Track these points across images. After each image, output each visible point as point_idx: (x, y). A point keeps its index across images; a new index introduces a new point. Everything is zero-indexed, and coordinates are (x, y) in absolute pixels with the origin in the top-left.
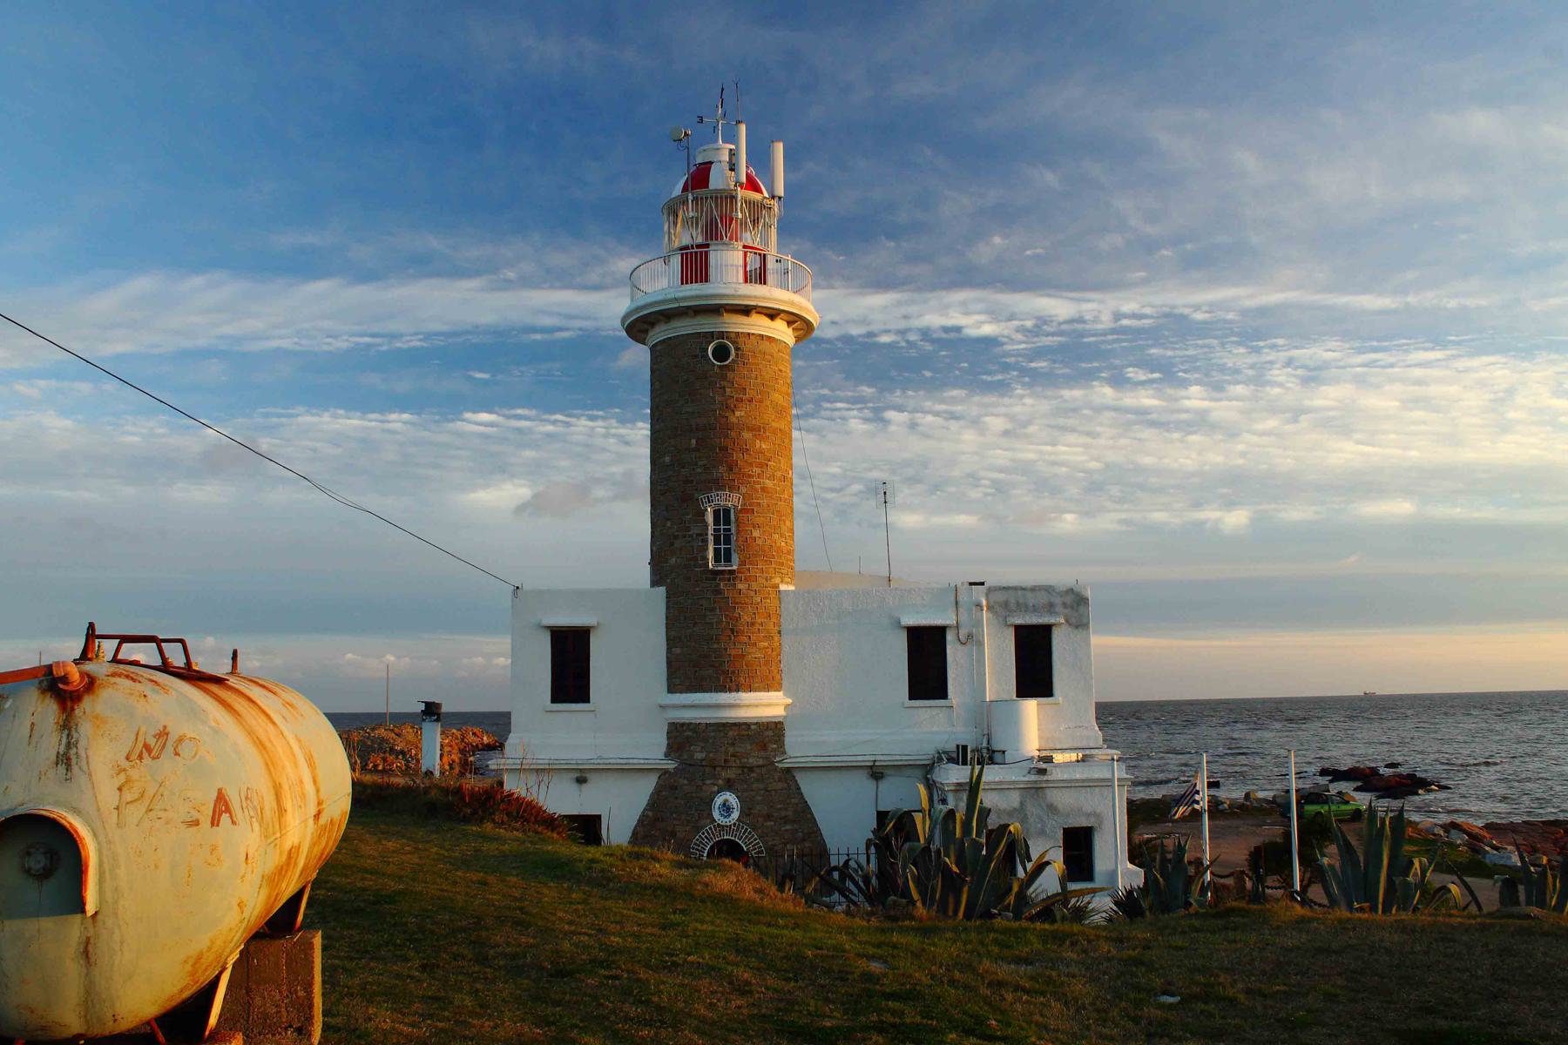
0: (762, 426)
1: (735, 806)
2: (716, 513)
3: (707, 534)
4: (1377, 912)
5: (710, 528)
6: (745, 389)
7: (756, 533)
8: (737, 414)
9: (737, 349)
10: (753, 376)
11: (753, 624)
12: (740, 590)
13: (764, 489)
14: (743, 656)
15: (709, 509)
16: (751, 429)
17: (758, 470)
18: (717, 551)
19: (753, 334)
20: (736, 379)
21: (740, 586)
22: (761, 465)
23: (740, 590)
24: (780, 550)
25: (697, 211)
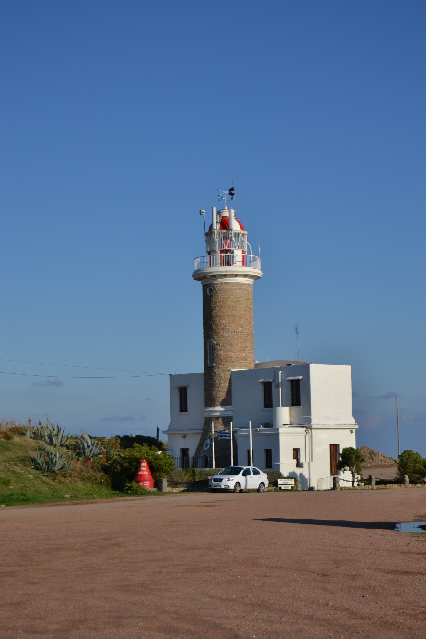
0: (223, 315)
1: (209, 444)
2: (210, 346)
3: (208, 354)
4: (212, 467)
5: (208, 352)
6: (216, 303)
7: (220, 353)
8: (214, 312)
9: (214, 289)
10: (220, 298)
11: (220, 384)
12: (216, 372)
13: (224, 337)
14: (216, 394)
15: (208, 345)
16: (218, 317)
17: (221, 331)
18: (210, 359)
19: (219, 283)
20: (214, 300)
21: (215, 371)
22: (222, 329)
23: (216, 372)
24: (231, 357)
25: (218, 239)
